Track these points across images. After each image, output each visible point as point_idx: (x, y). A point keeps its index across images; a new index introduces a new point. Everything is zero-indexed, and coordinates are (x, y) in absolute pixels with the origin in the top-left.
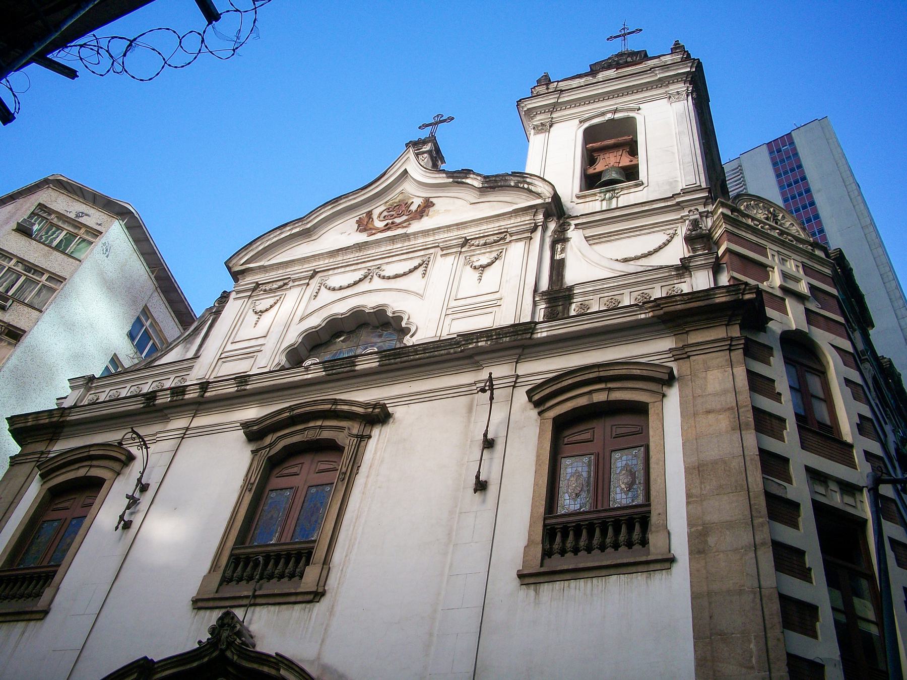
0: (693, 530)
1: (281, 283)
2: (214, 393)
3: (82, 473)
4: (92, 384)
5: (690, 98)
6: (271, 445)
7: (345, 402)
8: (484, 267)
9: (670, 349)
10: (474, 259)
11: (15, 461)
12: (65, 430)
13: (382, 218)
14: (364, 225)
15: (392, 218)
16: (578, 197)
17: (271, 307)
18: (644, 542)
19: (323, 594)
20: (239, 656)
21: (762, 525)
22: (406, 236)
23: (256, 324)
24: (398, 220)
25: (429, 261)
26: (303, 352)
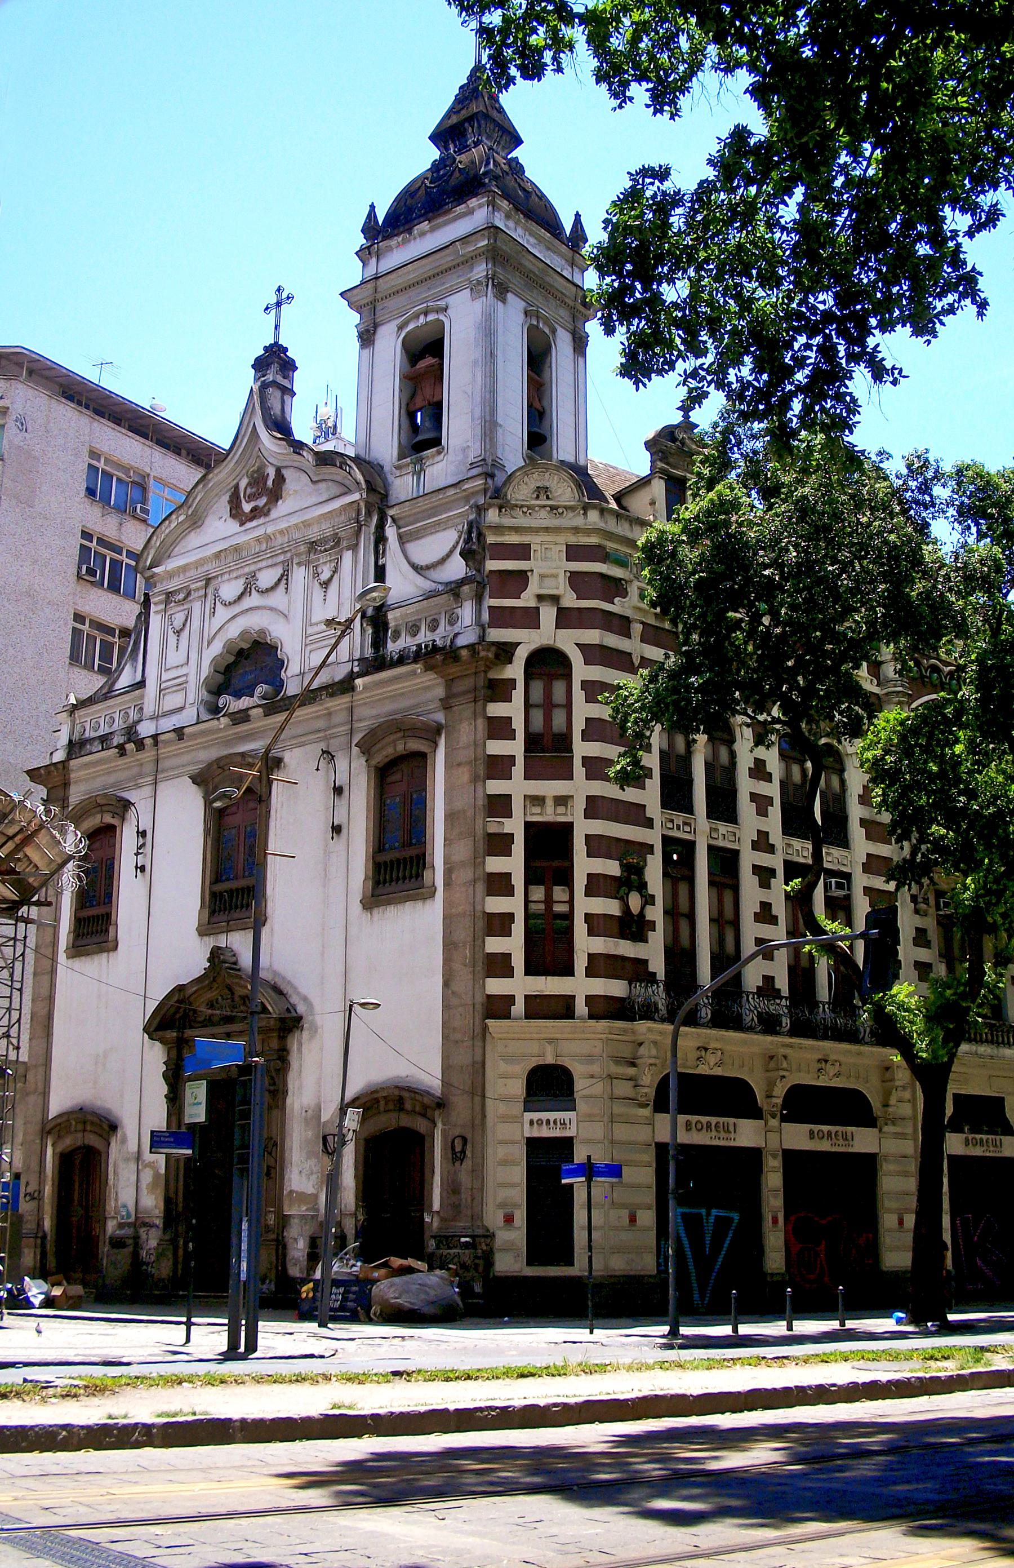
21: (479, 864)
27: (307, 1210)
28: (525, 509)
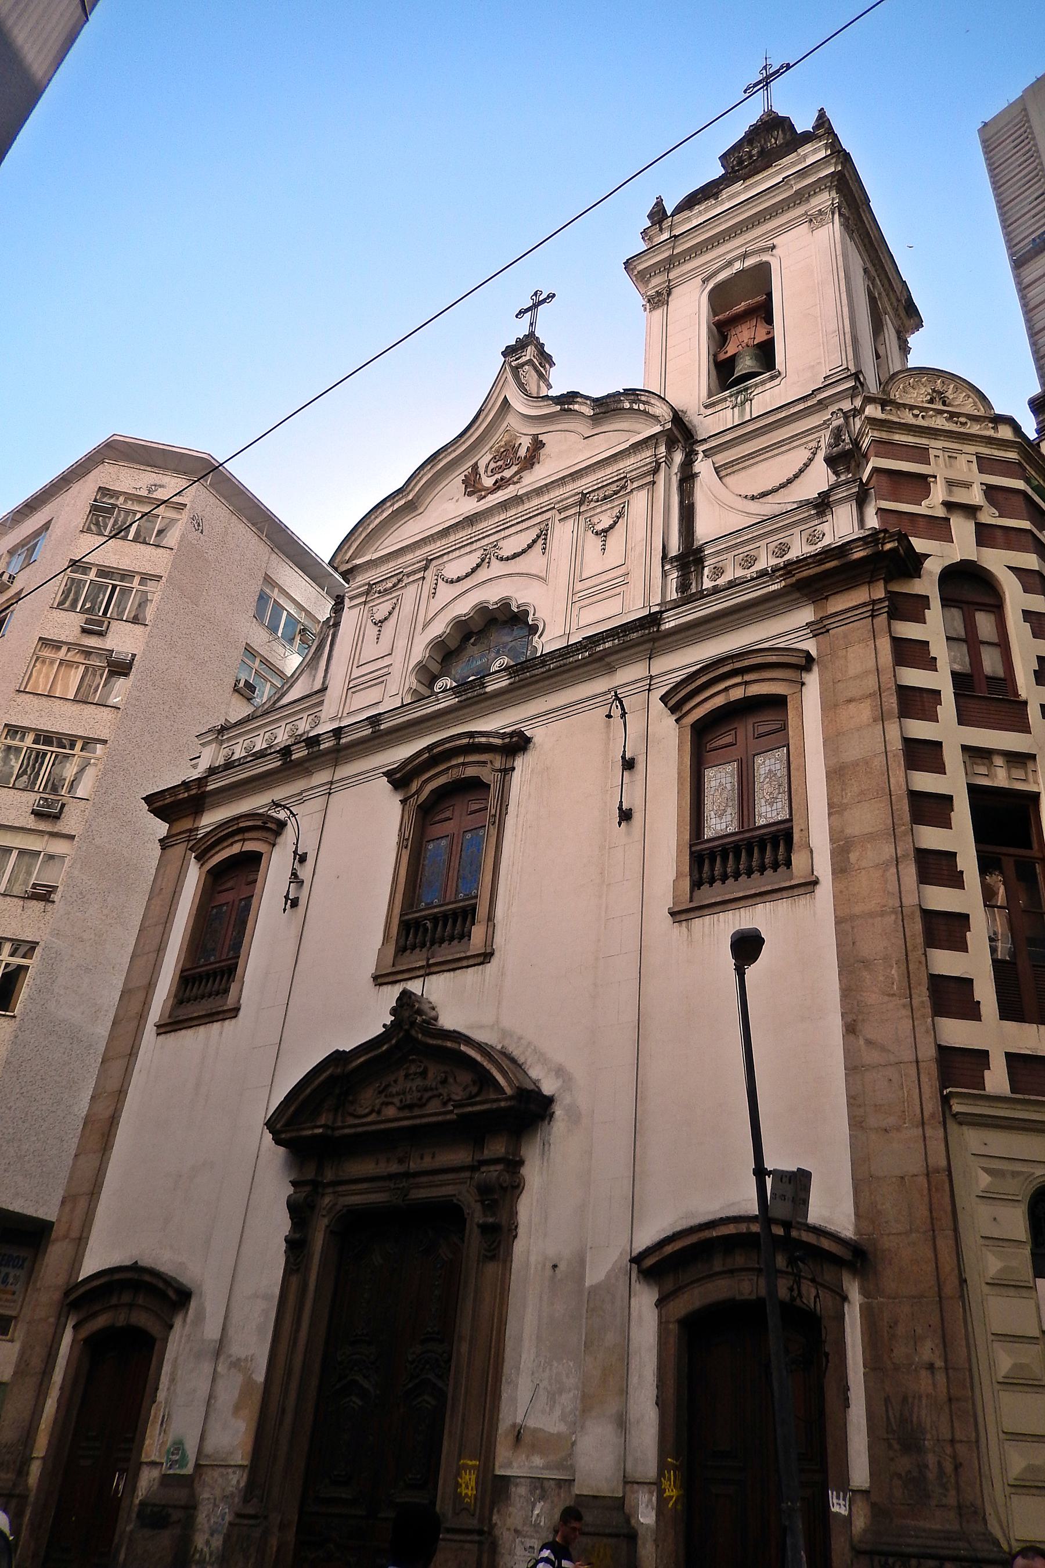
0: (835, 845)
1: (394, 580)
2: (349, 739)
3: (236, 849)
4: (222, 736)
5: (836, 216)
6: (418, 792)
7: (482, 734)
8: (605, 531)
9: (807, 624)
10: (595, 520)
11: (165, 843)
12: (207, 800)
13: (490, 474)
14: (472, 486)
15: (500, 471)
16: (706, 407)
17: (390, 613)
18: (788, 864)
19: (492, 954)
20: (423, 1034)
21: (905, 834)
22: (518, 500)
23: (378, 639)
24: (507, 474)
25: (547, 530)
26: (435, 668)
27: (547, 1467)
28: (916, 412)
